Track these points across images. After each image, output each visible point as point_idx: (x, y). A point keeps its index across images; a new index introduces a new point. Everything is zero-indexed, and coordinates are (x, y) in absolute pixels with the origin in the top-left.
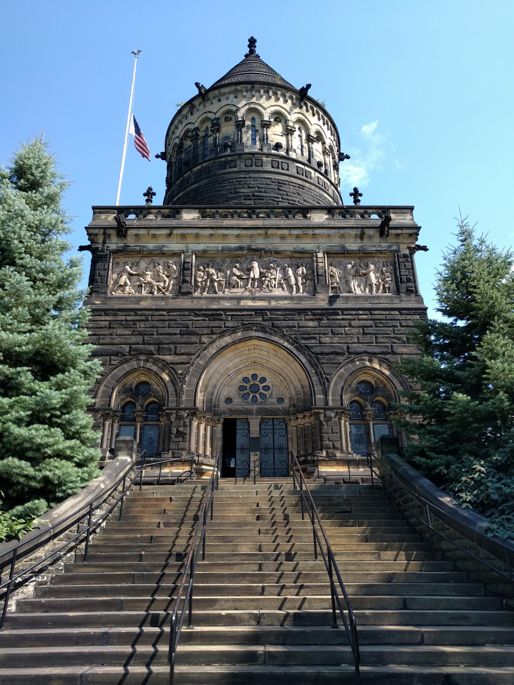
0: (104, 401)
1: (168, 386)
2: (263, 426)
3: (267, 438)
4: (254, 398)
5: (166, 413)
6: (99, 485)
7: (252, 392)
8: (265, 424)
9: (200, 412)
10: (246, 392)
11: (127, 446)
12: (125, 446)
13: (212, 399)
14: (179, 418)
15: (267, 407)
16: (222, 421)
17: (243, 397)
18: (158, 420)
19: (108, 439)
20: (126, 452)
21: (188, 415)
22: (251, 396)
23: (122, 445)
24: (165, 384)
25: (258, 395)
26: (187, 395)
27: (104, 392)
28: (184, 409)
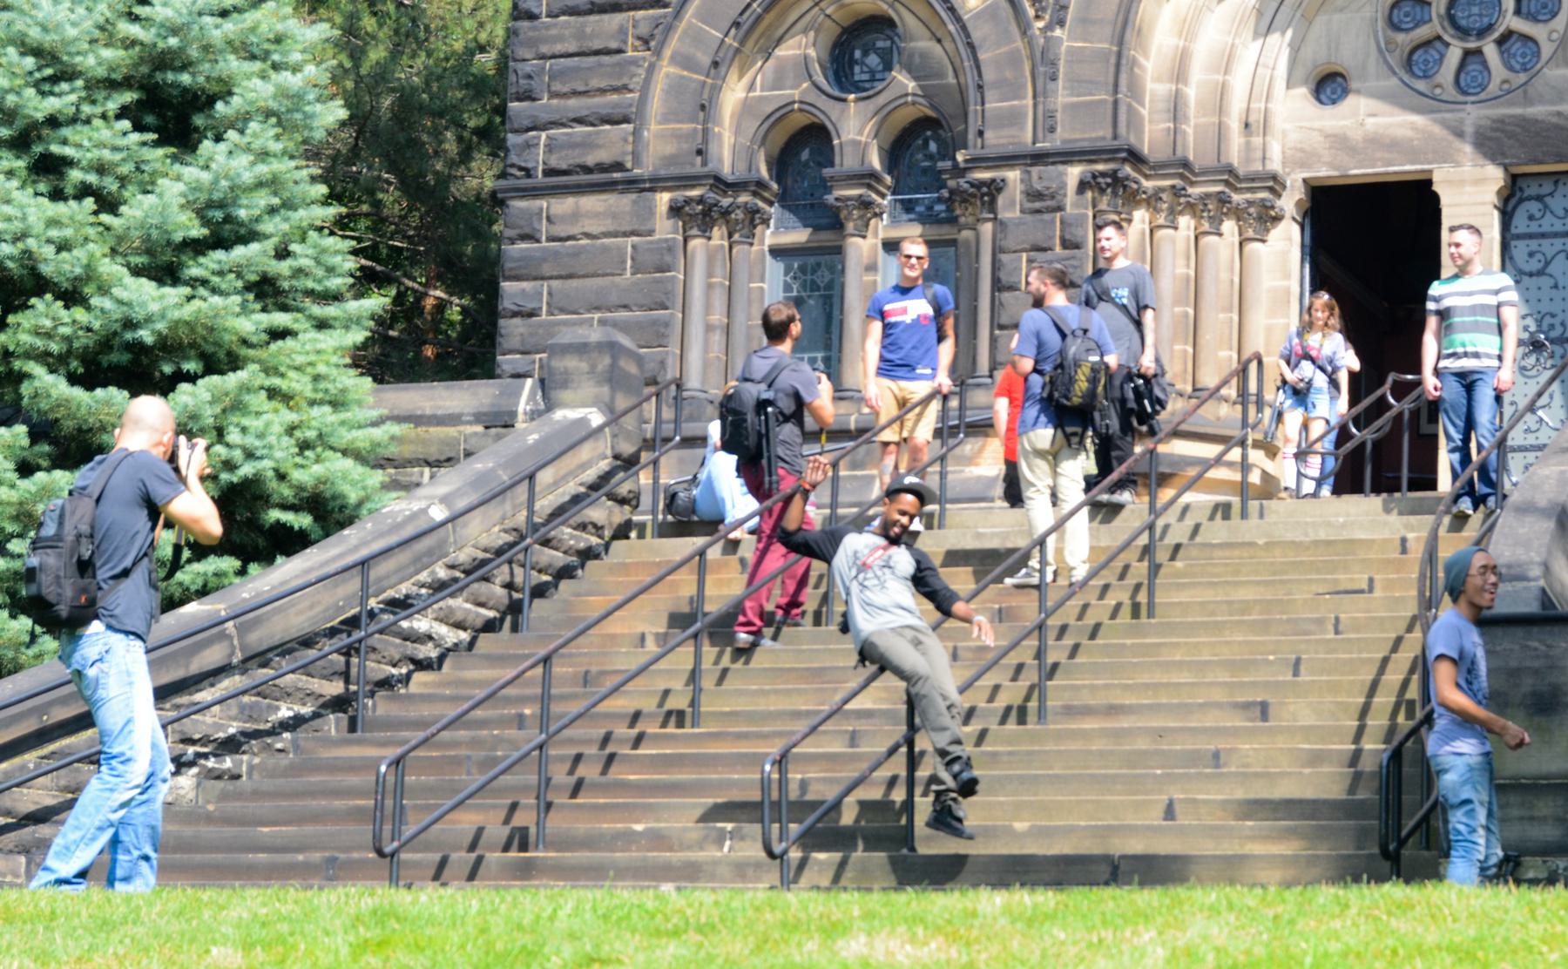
0: (677, 136)
1: (976, 36)
2: (1520, 224)
3: (1545, 282)
4: (1473, 67)
5: (978, 185)
6: (424, 511)
7: (1463, 32)
8: (1534, 207)
9: (1158, 169)
10: (1423, 32)
11: (592, 371)
12: (584, 366)
13: (1223, 91)
14: (1042, 201)
15: (1537, 111)
16: (1290, 202)
17: (1409, 64)
18: (952, 220)
19: (709, 328)
20: (589, 389)
21: (1083, 186)
22: (1454, 55)
23: (571, 363)
24: (964, 28)
25: (1490, 51)
26: (1076, 84)
27: (676, 89)
28: (1068, 156)
